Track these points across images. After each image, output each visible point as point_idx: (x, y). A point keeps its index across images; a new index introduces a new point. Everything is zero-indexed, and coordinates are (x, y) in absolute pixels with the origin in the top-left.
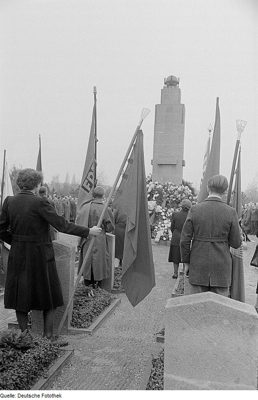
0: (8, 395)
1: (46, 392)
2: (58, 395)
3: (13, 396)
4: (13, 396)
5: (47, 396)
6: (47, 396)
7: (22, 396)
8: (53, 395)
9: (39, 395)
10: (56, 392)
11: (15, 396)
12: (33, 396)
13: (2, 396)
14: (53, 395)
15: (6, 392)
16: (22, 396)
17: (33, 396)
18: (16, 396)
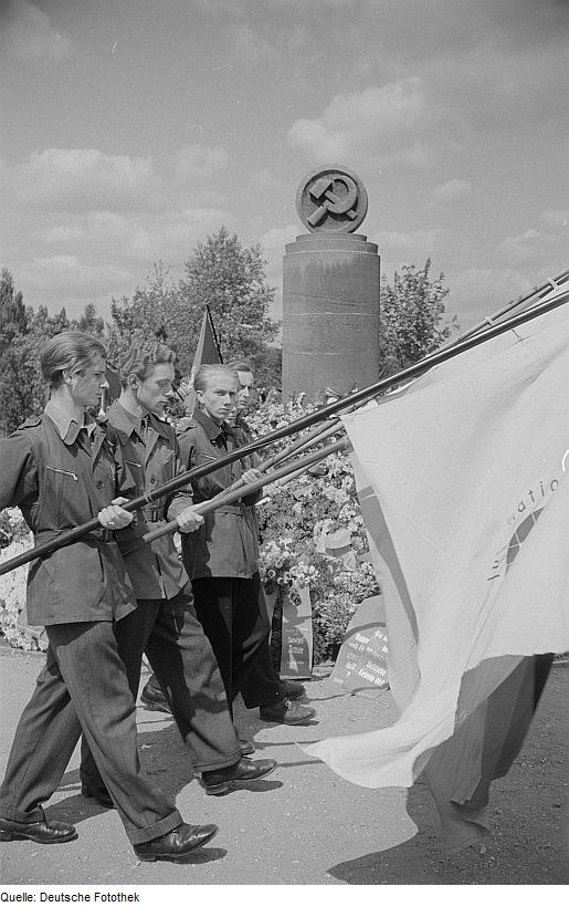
0: (19, 897)
1: (104, 889)
2: (130, 897)
3: (29, 898)
4: (29, 898)
5: (108, 898)
6: (108, 898)
7: (50, 898)
8: (120, 897)
9: (88, 897)
10: (128, 890)
11: (34, 898)
12: (75, 898)
13: (4, 897)
14: (120, 897)
15: (14, 890)
16: (50, 898)
17: (75, 898)
18: (37, 898)
